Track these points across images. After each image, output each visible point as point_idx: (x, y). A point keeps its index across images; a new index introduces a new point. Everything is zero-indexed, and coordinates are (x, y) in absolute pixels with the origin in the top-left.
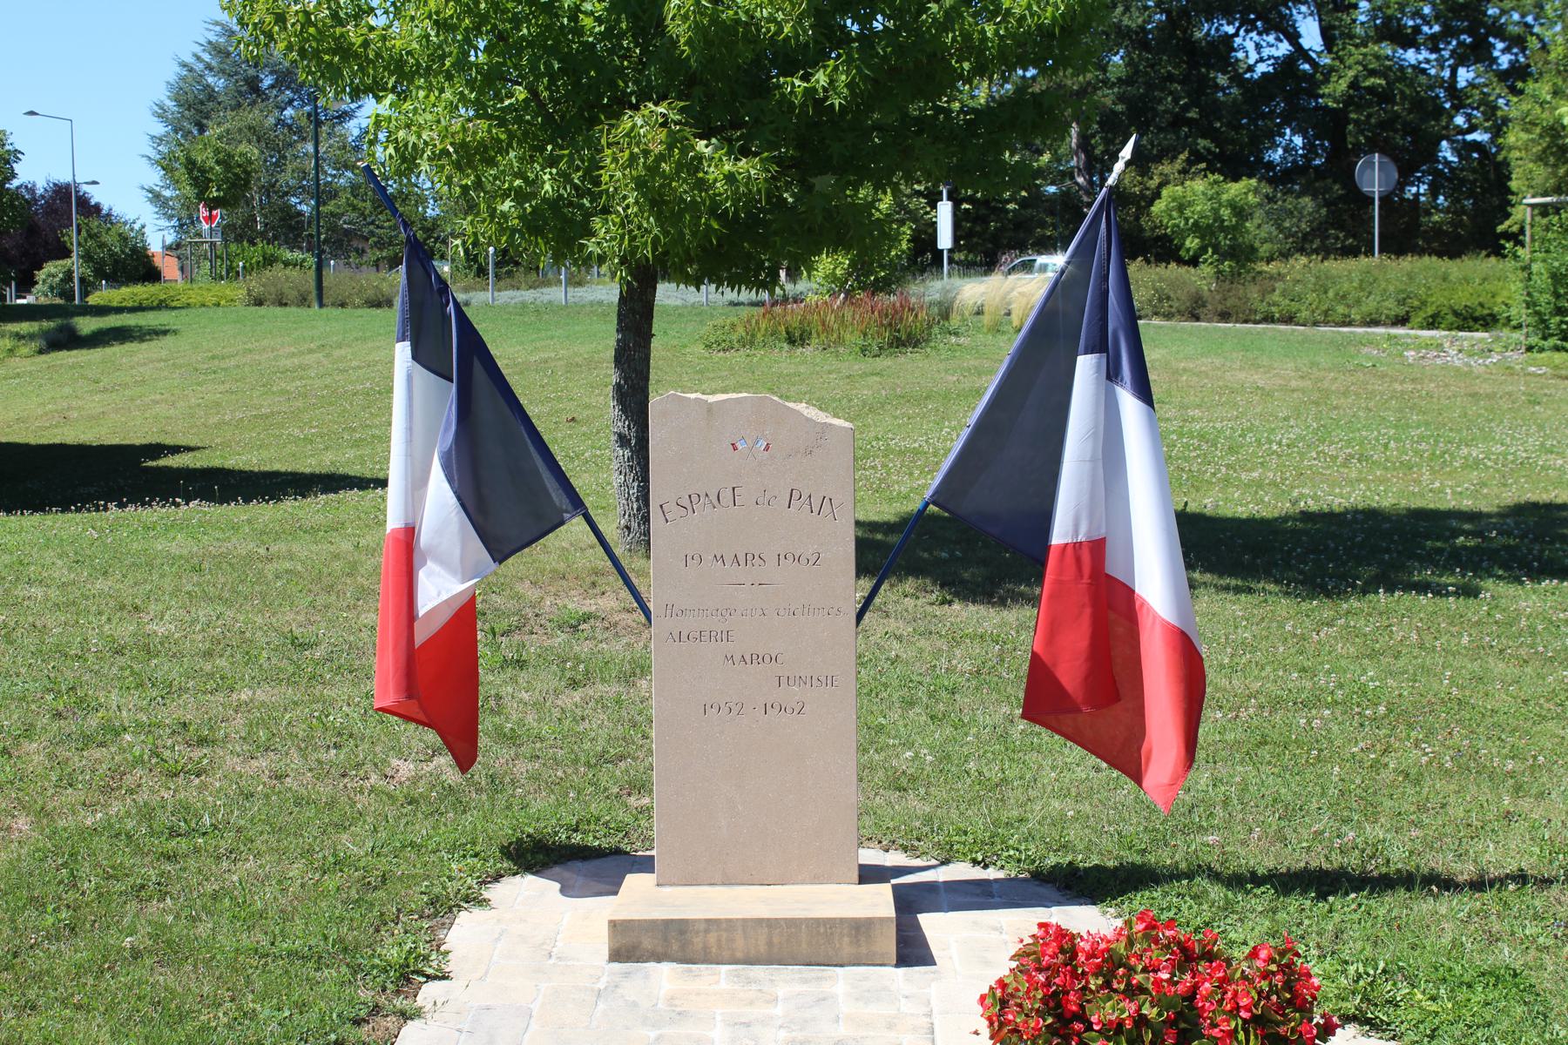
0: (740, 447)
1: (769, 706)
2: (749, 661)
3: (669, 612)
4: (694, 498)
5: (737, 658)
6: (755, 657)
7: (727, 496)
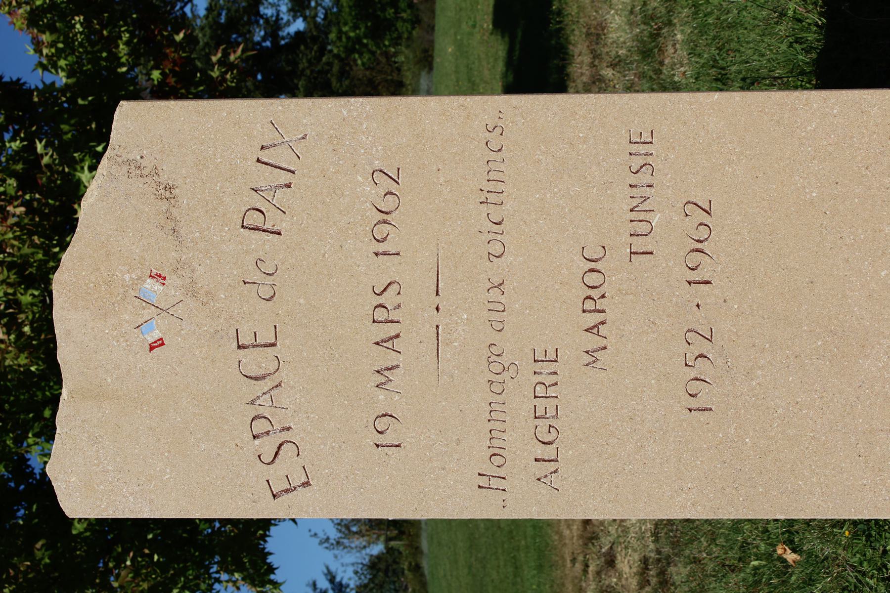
0: (157, 335)
1: (695, 276)
2: (598, 317)
3: (494, 483)
4: (260, 426)
5: (593, 341)
6: (589, 305)
7: (256, 362)
